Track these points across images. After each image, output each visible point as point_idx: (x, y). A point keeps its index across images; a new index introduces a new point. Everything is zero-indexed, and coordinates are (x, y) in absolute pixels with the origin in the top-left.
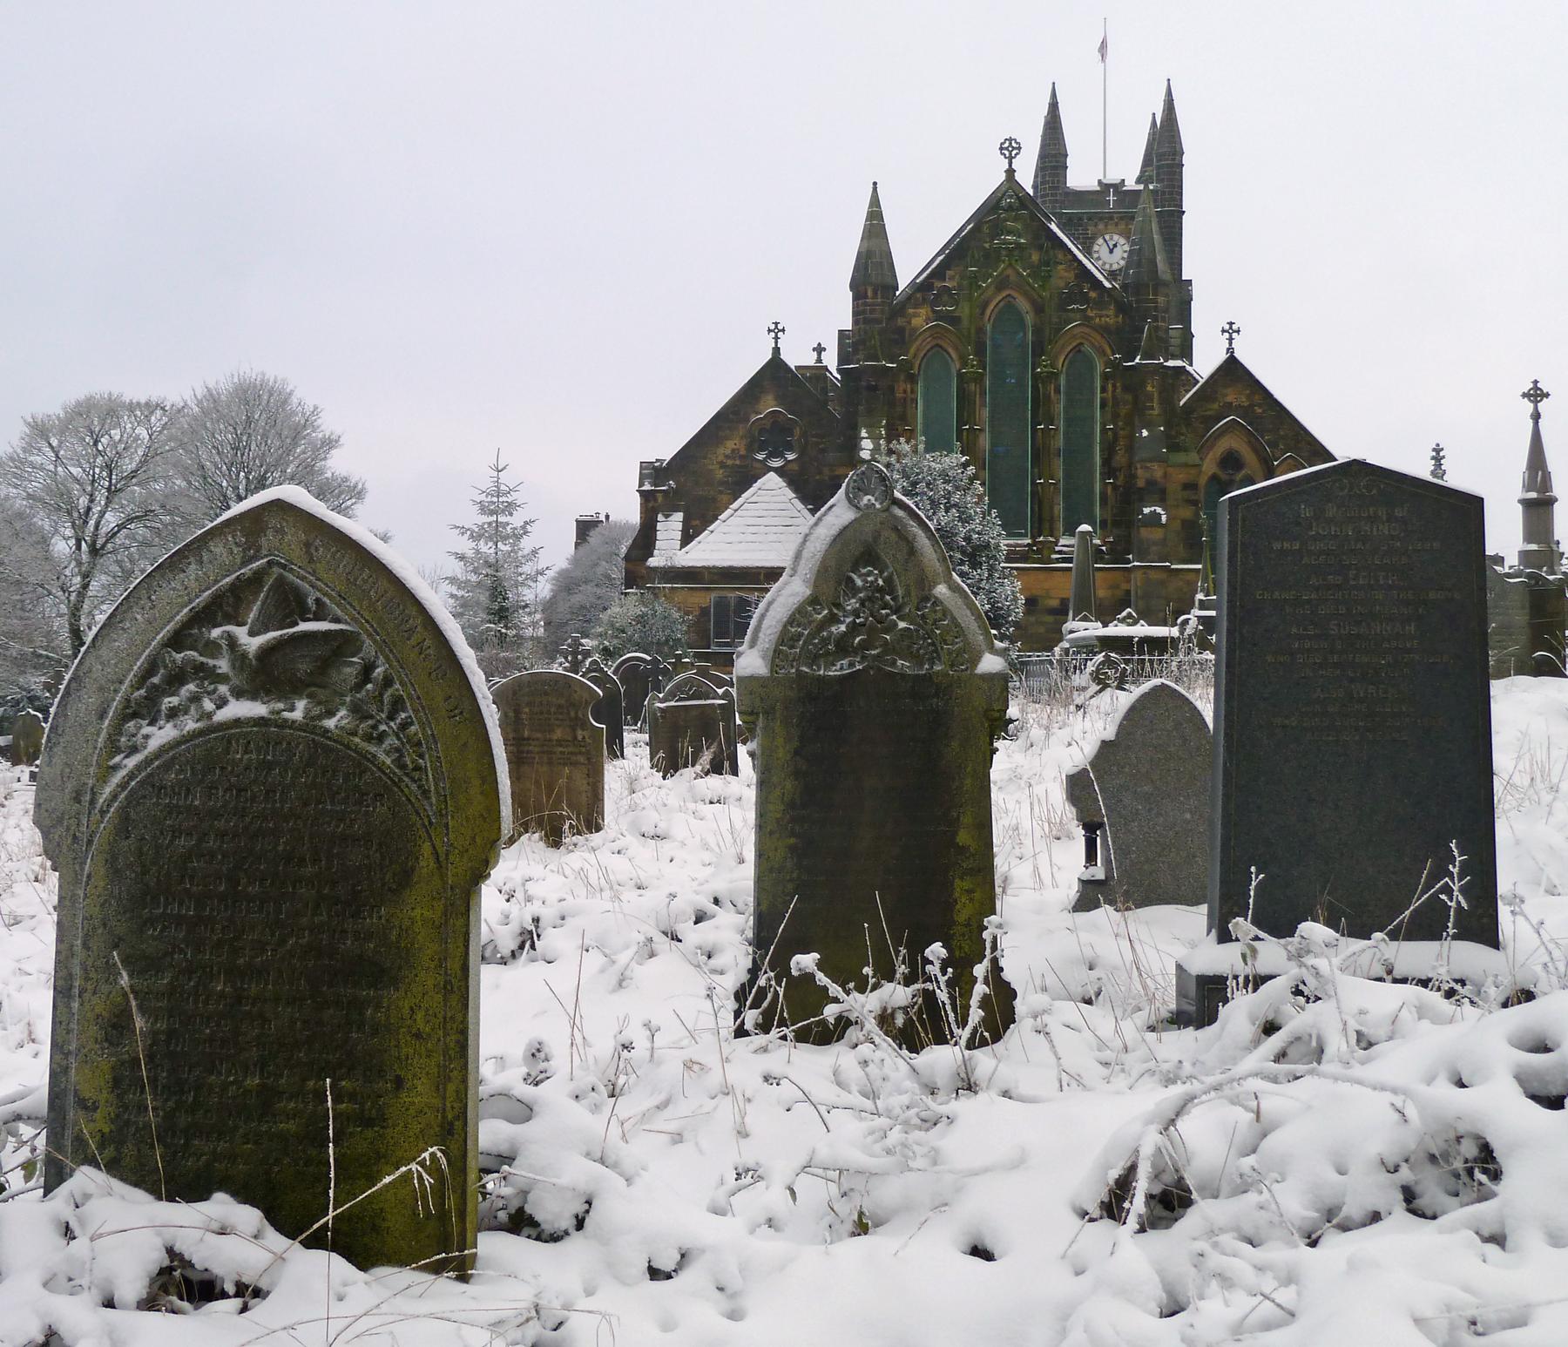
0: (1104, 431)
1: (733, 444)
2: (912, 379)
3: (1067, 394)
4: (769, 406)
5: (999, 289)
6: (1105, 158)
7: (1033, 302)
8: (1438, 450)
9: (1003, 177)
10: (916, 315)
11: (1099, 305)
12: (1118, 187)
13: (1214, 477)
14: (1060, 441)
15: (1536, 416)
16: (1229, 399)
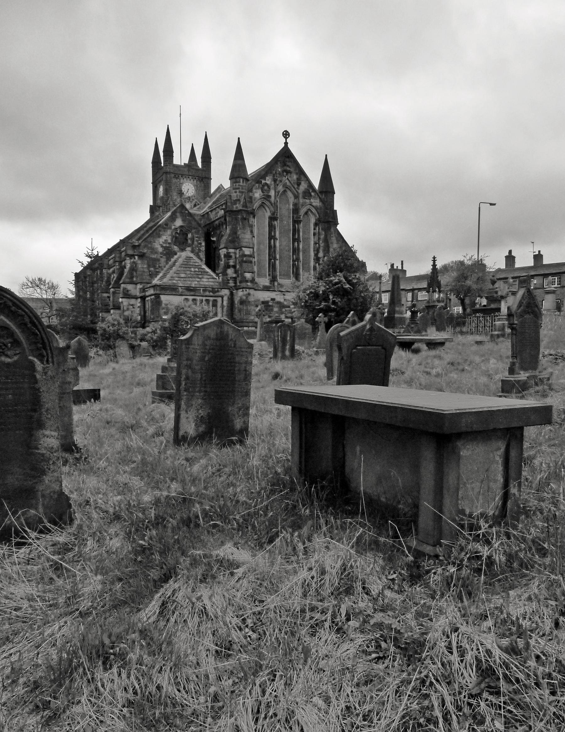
0: (315, 243)
8: (434, 258)
9: (283, 145)
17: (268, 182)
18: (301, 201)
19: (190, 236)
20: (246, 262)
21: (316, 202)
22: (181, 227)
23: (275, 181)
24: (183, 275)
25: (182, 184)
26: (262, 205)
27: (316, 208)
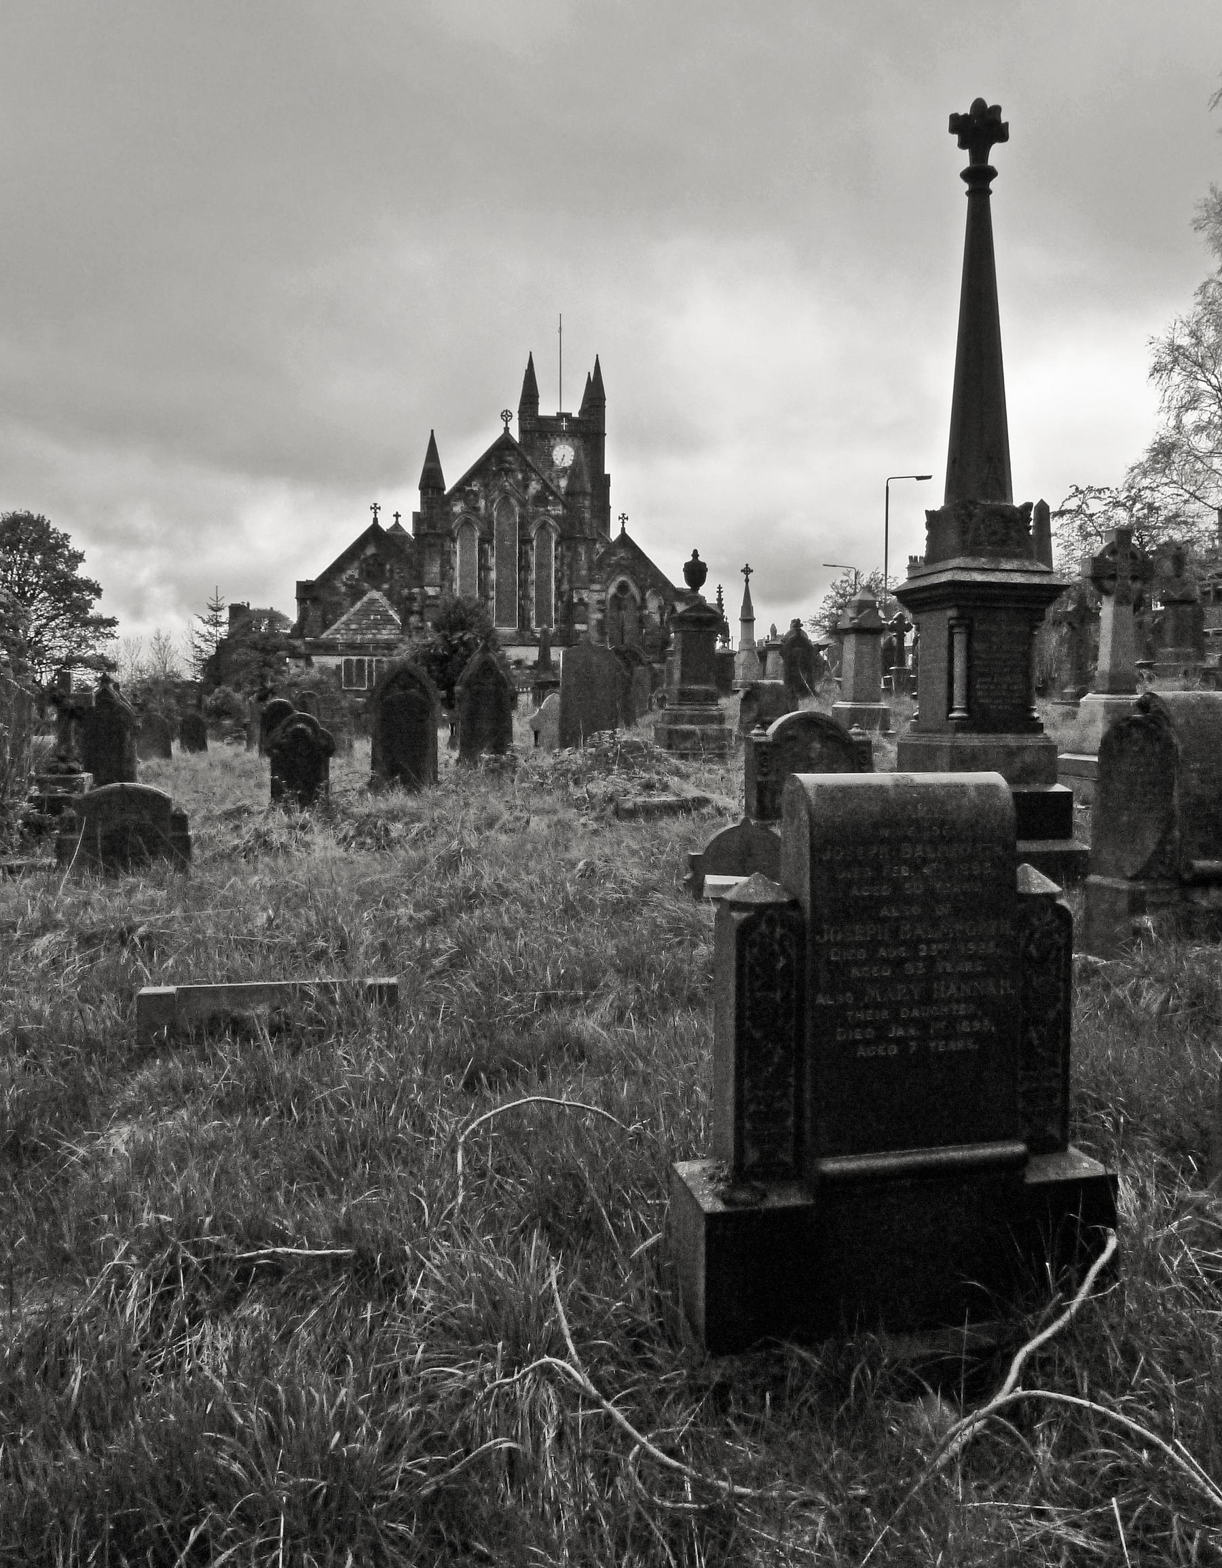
0: (557, 571)
1: (353, 572)
4: (370, 550)
11: (555, 504)
12: (568, 416)
13: (615, 596)
15: (747, 581)
17: (475, 489)
18: (530, 508)
19: (388, 567)
20: (428, 606)
21: (559, 511)
22: (373, 555)
23: (486, 486)
24: (353, 627)
25: (553, 447)
26: (467, 523)
27: (556, 518)
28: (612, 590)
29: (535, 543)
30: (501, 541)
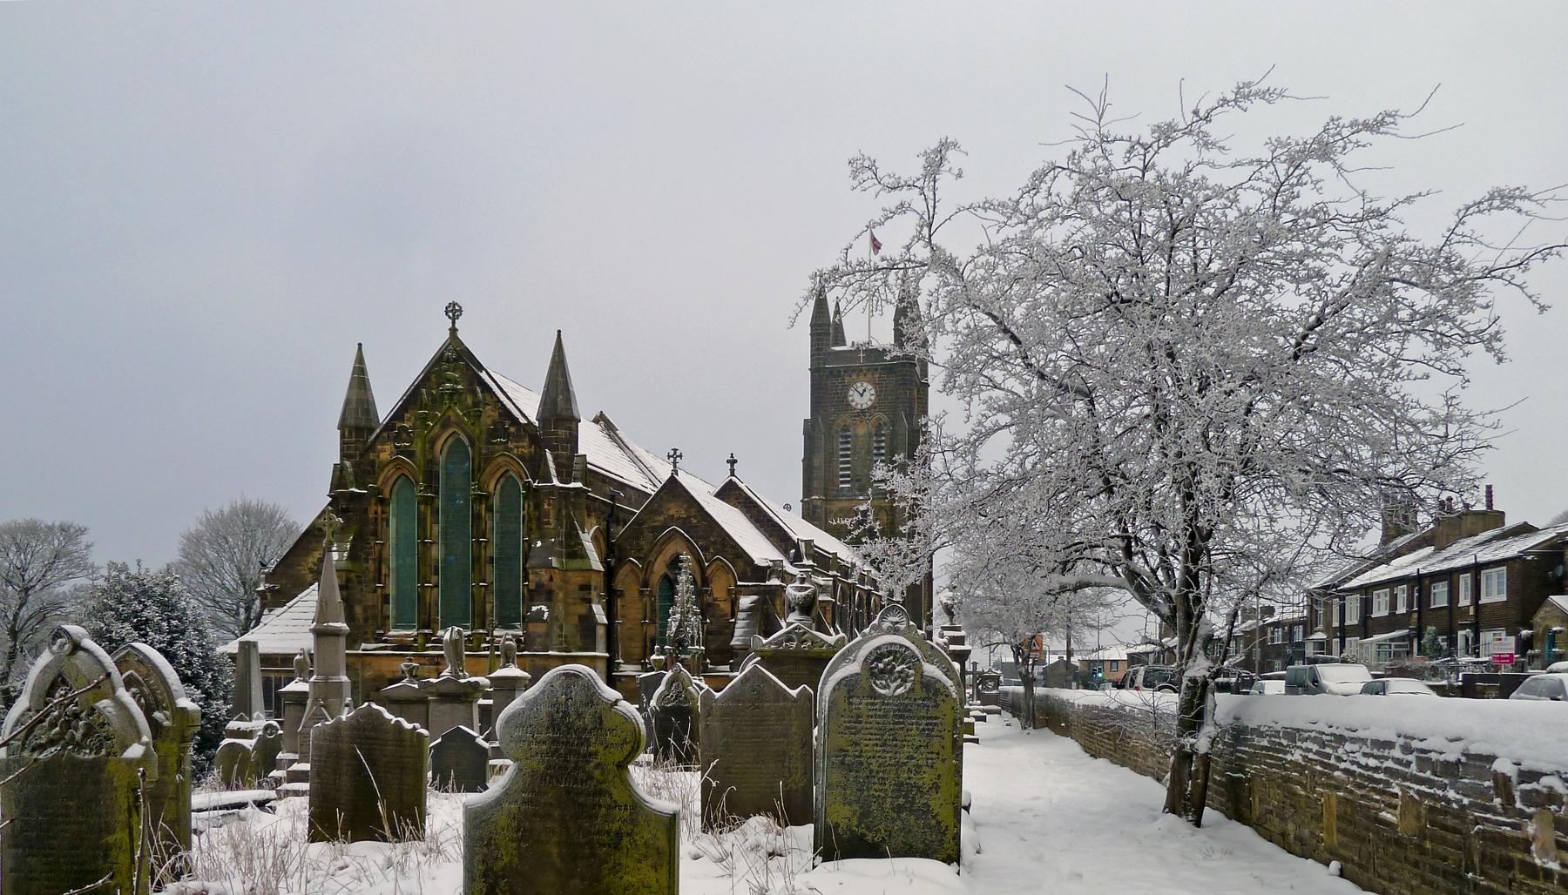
2: (383, 502)
3: (501, 512)
5: (445, 426)
6: (870, 327)
7: (469, 438)
10: (383, 451)
13: (665, 576)
14: (493, 551)
16: (672, 512)
25: (847, 387)
28: (659, 568)
29: (496, 501)
30: (450, 499)
